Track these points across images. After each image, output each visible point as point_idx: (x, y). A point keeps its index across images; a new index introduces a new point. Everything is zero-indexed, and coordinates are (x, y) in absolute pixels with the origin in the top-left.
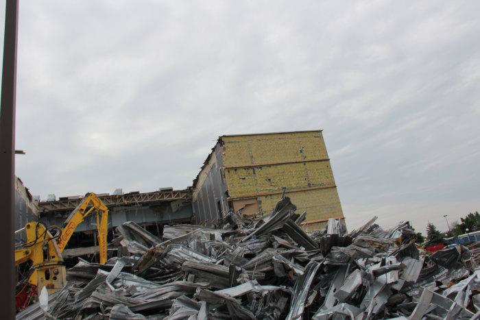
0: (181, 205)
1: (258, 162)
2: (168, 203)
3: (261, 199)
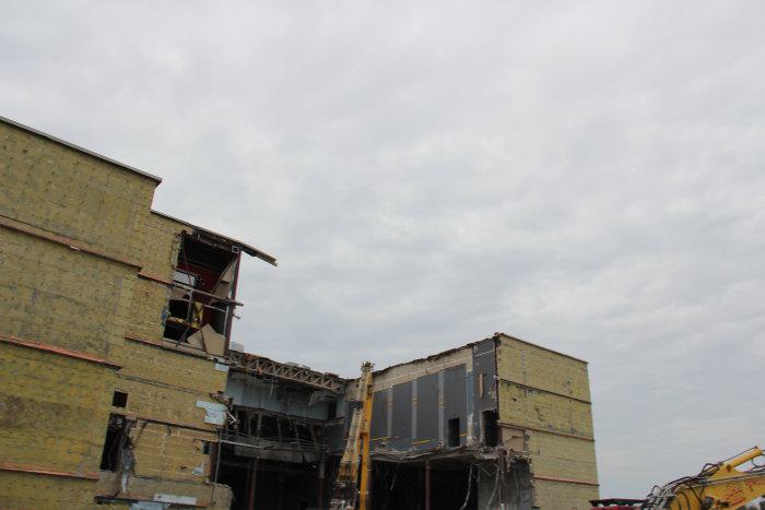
0: (322, 399)
1: (530, 383)
2: (312, 389)
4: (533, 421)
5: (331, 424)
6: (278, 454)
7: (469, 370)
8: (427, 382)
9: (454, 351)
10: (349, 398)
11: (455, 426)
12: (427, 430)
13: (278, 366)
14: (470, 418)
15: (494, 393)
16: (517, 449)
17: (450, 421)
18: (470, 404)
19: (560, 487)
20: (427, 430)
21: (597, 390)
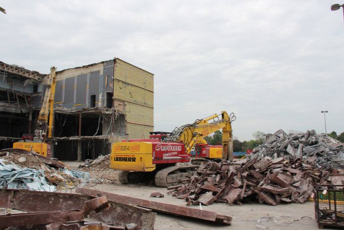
2: (26, 78)
3: (126, 103)
4: (127, 98)
5: (35, 95)
6: (8, 109)
7: (102, 73)
8: (82, 77)
9: (95, 64)
10: (44, 83)
11: (93, 98)
12: (81, 99)
13: (7, 66)
14: (101, 95)
15: (112, 85)
16: (121, 110)
17: (91, 96)
18: (101, 89)
19: (138, 126)
20: (81, 99)
21: (156, 87)
